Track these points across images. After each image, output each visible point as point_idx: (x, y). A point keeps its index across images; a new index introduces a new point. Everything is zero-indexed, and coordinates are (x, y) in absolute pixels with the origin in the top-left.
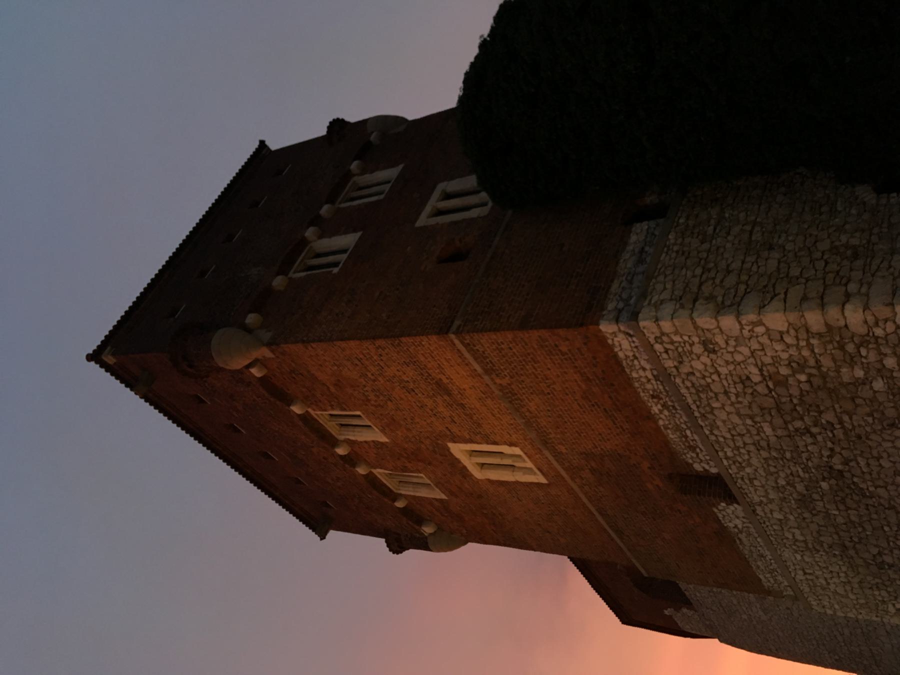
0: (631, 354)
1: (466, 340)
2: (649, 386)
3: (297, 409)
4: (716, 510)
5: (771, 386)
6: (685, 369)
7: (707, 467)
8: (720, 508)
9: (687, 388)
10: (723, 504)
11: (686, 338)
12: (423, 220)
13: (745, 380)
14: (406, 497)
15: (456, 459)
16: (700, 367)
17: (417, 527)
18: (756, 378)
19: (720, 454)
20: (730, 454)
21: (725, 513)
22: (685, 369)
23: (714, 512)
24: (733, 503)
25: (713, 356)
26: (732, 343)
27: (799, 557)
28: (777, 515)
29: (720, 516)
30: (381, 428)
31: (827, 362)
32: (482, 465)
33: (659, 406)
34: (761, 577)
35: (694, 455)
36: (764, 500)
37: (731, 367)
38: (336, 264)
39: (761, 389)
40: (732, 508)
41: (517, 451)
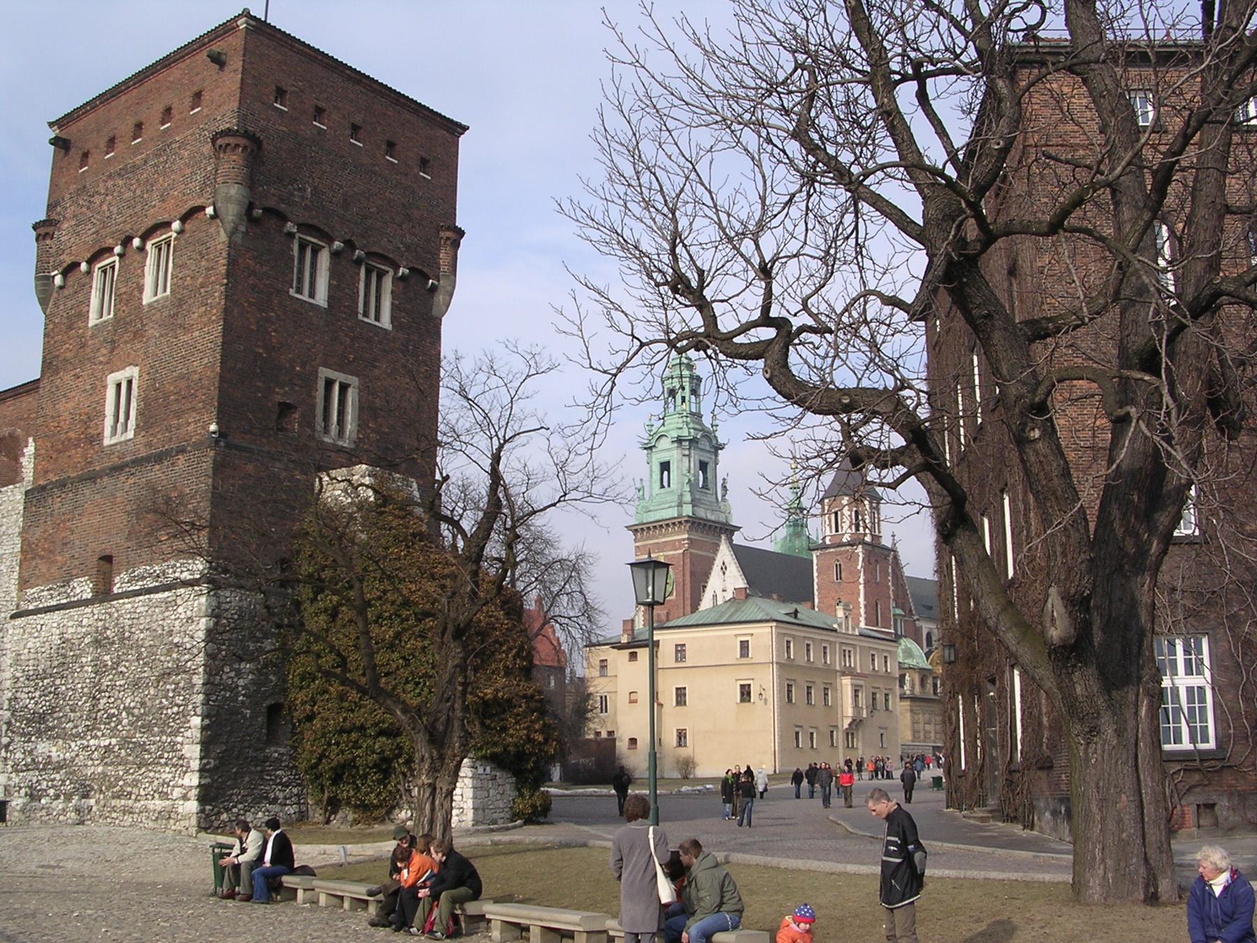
2: (171, 571)
3: (176, 225)
7: (118, 585)
10: (91, 585)
12: (325, 372)
13: (170, 633)
14: (89, 272)
15: (123, 368)
17: (61, 269)
19: (126, 600)
20: (127, 606)
27: (55, 625)
28: (85, 622)
29: (82, 579)
32: (119, 386)
34: (34, 590)
36: (96, 617)
38: (299, 291)
40: (89, 590)
41: (130, 434)
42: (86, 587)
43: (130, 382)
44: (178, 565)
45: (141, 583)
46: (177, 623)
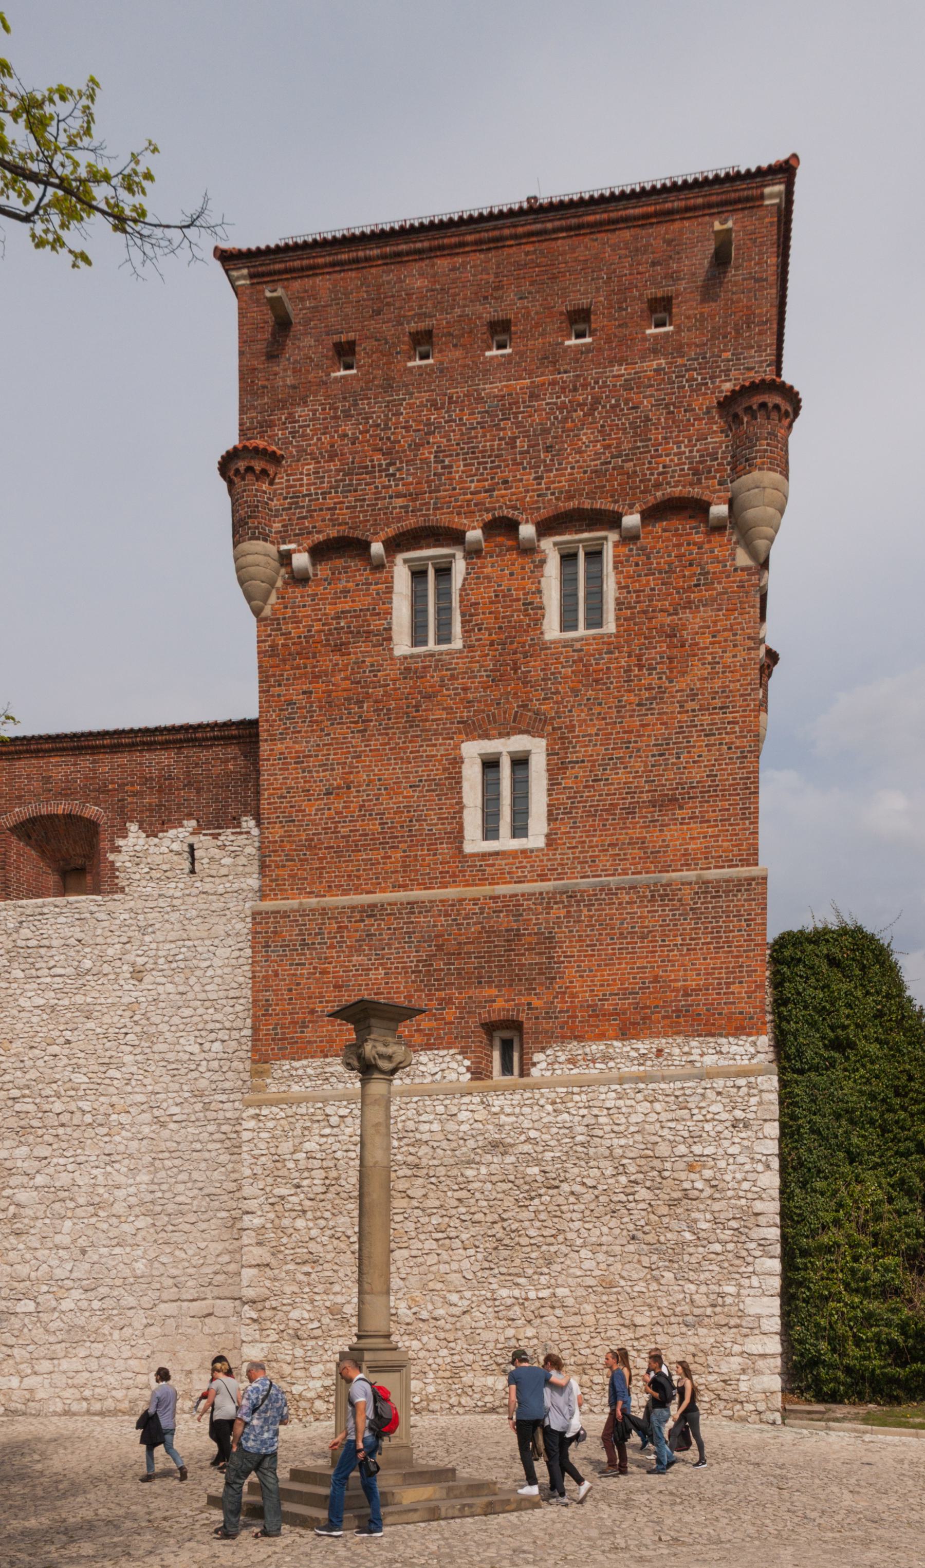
0: (724, 1050)
1: (757, 884)
4: (452, 1051)
5: (685, 1159)
6: (710, 1094)
8: (459, 1057)
9: (683, 1088)
11: (754, 1109)
16: (713, 1108)
18: (697, 1149)
19: (576, 1090)
20: (576, 1098)
21: (447, 1059)
22: (710, 1094)
23: (449, 1048)
24: (472, 1073)
25: (728, 1124)
26: (746, 1143)
30: (578, 646)
31: (716, 1206)
33: (642, 1051)
35: (562, 1058)
37: (712, 1133)
39: (682, 1149)
42: (454, 1065)
43: (520, 762)
44: (694, 1044)
45: (598, 1065)
46: (708, 1127)
